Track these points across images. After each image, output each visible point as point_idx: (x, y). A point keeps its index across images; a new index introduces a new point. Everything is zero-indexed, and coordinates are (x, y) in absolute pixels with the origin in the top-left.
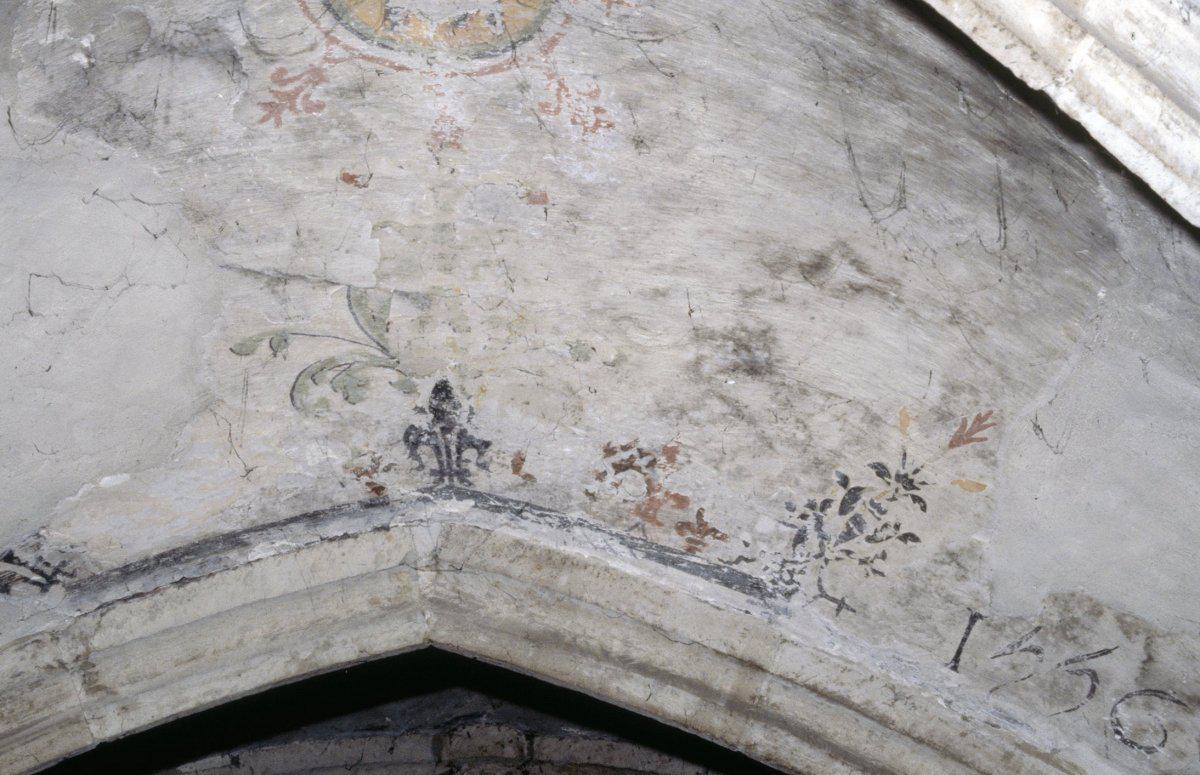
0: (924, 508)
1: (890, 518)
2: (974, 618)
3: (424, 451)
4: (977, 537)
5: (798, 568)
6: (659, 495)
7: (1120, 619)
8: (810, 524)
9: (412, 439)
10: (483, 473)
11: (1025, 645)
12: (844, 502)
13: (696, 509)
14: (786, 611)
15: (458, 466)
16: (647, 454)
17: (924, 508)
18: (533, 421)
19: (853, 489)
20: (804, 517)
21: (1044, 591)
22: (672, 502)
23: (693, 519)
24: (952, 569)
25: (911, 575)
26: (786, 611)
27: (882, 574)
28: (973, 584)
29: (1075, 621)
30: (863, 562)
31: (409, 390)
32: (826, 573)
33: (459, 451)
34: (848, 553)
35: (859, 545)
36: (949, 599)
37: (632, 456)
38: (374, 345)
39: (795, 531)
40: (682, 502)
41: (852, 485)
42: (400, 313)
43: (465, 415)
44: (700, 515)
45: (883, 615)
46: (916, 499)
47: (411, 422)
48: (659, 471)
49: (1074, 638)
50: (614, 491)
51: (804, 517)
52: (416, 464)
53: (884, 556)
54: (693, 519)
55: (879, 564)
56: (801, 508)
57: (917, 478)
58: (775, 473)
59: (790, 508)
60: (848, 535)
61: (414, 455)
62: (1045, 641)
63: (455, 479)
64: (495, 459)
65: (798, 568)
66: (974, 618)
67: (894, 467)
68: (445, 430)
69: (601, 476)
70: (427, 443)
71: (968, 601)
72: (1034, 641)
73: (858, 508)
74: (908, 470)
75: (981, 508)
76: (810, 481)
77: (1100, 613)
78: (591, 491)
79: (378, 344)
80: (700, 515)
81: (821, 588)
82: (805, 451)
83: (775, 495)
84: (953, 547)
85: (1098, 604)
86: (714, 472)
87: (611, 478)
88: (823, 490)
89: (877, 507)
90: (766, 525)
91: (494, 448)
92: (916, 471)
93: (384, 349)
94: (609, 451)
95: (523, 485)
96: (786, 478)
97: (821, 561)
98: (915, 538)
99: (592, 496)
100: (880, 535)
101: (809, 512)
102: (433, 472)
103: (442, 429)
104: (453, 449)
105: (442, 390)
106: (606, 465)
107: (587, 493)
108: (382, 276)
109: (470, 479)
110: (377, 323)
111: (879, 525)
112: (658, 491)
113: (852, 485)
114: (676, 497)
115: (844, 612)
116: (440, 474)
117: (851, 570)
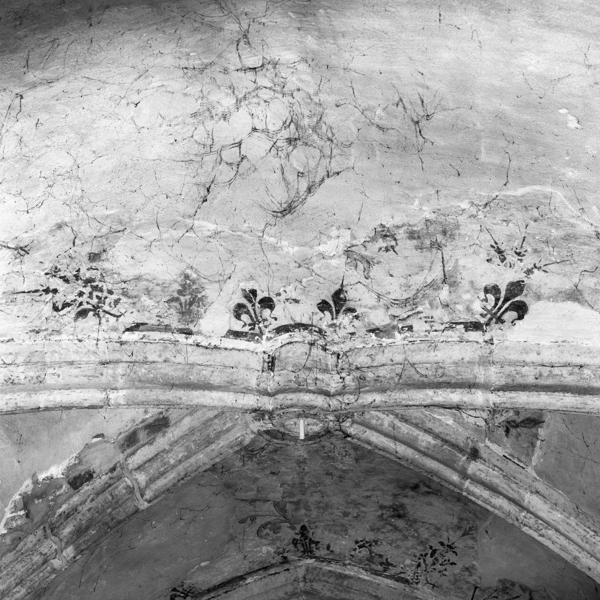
0: (457, 555)
1: (446, 558)
2: (476, 588)
4: (474, 563)
5: (419, 575)
7: (521, 586)
11: (492, 596)
14: (417, 589)
17: (457, 555)
21: (497, 579)
24: (467, 573)
25: (455, 575)
26: (417, 589)
27: (446, 575)
28: (474, 577)
29: (507, 587)
30: (439, 572)
32: (428, 576)
34: (435, 569)
35: (438, 567)
36: (467, 582)
45: (447, 588)
46: (454, 552)
49: (507, 593)
53: (446, 570)
55: (445, 572)
57: (454, 546)
60: (434, 564)
62: (498, 593)
65: (419, 575)
66: (476, 588)
67: (446, 543)
71: (473, 582)
72: (495, 594)
73: (436, 555)
74: (450, 543)
75: (474, 554)
77: (514, 585)
81: (427, 580)
84: (467, 566)
85: (513, 582)
88: (424, 550)
89: (442, 555)
92: (453, 544)
97: (426, 572)
98: (455, 564)
100: (444, 563)
111: (443, 560)
115: (435, 588)
117: (436, 575)
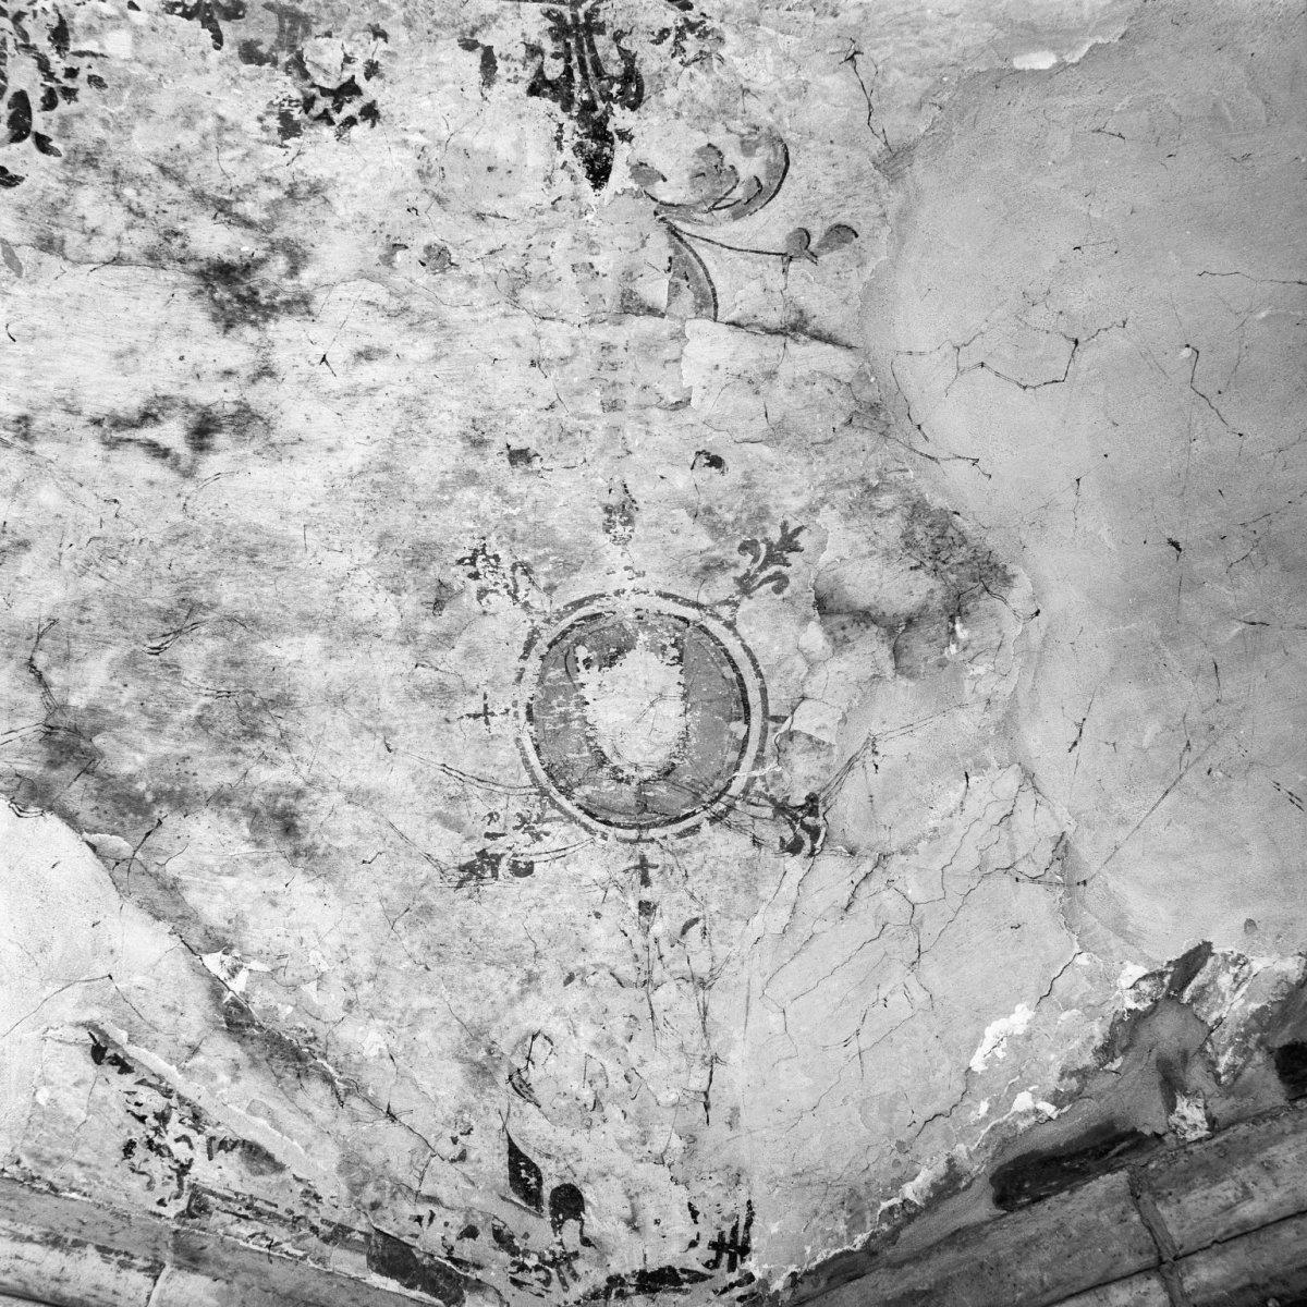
3: (615, 69)
6: (284, 57)
8: (58, 65)
9: (632, 90)
10: (533, 39)
12: (28, 111)
13: (226, 47)
15: (567, 45)
16: (318, 118)
18: (479, 143)
19: (25, 137)
20: (72, 73)
22: (263, 49)
23: (225, 27)
31: (641, 171)
37: (338, 110)
38: (685, 237)
39: (73, 47)
40: (250, 53)
41: (29, 141)
42: (655, 289)
43: (567, 135)
44: (218, 39)
47: (634, 115)
48: (296, 95)
50: (348, 49)
51: (72, 73)
52: (624, 43)
54: (225, 27)
56: (80, 83)
58: (140, 129)
59: (95, 81)
61: (628, 57)
63: (569, 20)
64: (520, 67)
68: (589, 107)
69: (372, 70)
70: (612, 79)
76: (88, 132)
78: (380, 40)
79: (681, 240)
80: (218, 39)
82: (115, 173)
83: (127, 94)
86: (222, 112)
87: (357, 71)
88: (65, 123)
90: (117, 44)
91: (522, 88)
93: (673, 232)
94: (370, 112)
95: (474, 31)
96: (122, 126)
99: (379, 33)
101: (67, 83)
102: (601, 29)
103: (595, 108)
104: (577, 76)
105: (599, 173)
106: (371, 89)
107: (384, 35)
108: (679, 336)
109: (550, 24)
110: (684, 268)
112: (288, 64)
113: (29, 141)
114: (260, 60)
116: (592, 27)
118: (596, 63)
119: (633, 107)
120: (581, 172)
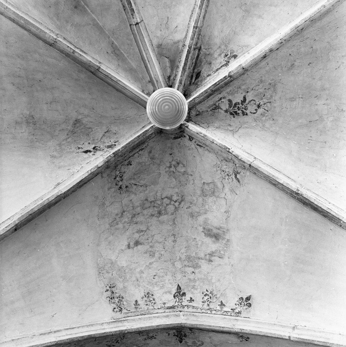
33: (178, 334)
116: (181, 331)
118: (181, 334)
119: (185, 337)
120: (179, 342)
